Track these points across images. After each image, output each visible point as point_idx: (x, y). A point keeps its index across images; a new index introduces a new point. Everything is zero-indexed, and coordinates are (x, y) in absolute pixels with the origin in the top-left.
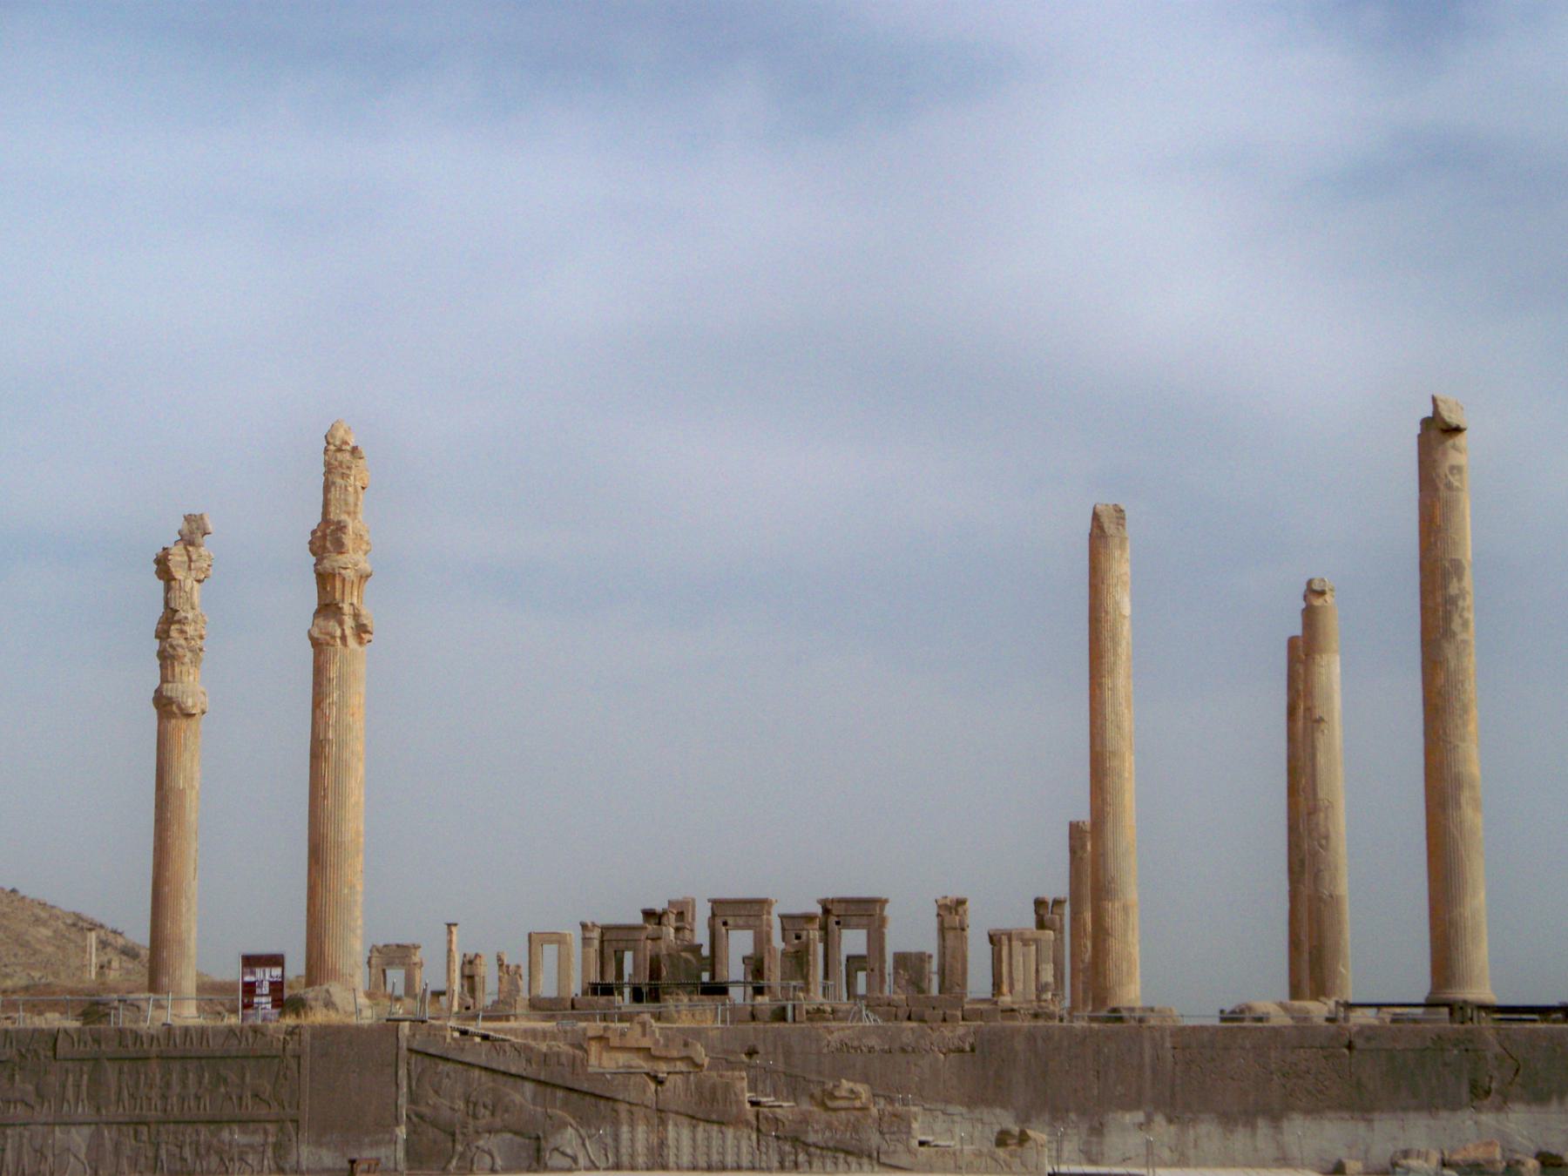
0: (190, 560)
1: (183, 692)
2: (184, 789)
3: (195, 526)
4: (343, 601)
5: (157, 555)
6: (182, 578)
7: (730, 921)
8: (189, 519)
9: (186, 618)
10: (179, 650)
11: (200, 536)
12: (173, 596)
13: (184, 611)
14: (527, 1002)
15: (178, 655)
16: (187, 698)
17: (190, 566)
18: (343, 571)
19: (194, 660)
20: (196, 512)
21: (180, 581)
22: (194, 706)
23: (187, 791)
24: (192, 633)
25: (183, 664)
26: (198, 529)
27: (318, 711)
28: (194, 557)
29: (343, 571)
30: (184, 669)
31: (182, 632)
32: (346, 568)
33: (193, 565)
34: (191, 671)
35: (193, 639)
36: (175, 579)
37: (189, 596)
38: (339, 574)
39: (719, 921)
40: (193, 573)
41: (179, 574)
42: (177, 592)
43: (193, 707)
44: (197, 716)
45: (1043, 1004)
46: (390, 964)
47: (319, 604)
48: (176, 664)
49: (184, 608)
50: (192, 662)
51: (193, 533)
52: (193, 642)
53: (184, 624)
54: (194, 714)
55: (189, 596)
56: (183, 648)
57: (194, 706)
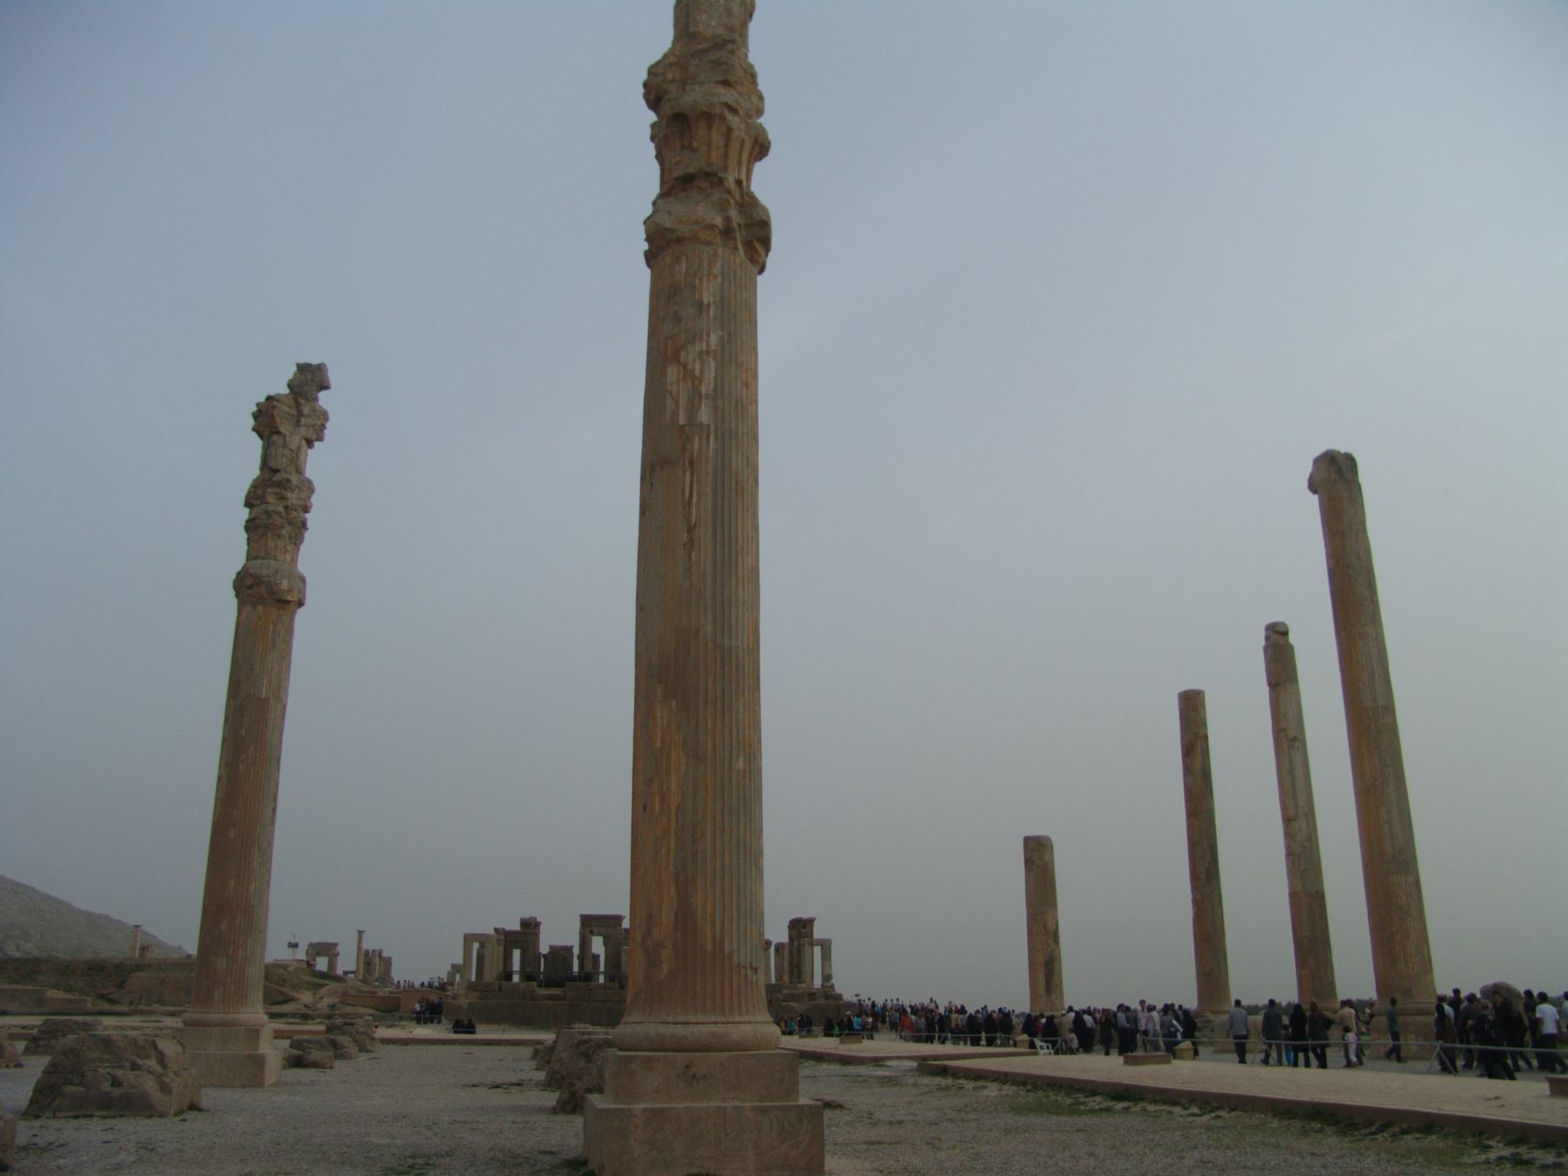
0: (300, 414)
1: (277, 571)
2: (267, 699)
3: (309, 377)
4: (725, 169)
5: (258, 405)
6: (287, 433)
7: (595, 930)
8: (303, 368)
9: (289, 481)
10: (276, 517)
11: (315, 388)
12: (274, 452)
13: (286, 472)
14: (466, 985)
15: (274, 524)
16: (282, 578)
17: (299, 421)
18: (729, 116)
19: (293, 534)
20: (314, 361)
21: (285, 436)
22: (290, 591)
23: (272, 703)
24: (295, 501)
25: (280, 537)
26: (312, 380)
27: (672, 372)
28: (306, 410)
29: (729, 116)
30: (280, 543)
31: (282, 498)
32: (734, 111)
33: (303, 420)
34: (289, 548)
35: (296, 510)
36: (278, 433)
37: (294, 455)
38: (722, 118)
39: (588, 930)
40: (303, 430)
41: (285, 428)
42: (280, 449)
43: (289, 591)
44: (292, 604)
45: (826, 989)
46: (320, 954)
47: (663, 183)
48: (270, 535)
49: (288, 469)
50: (290, 537)
51: (310, 380)
52: (294, 513)
53: (285, 489)
54: (288, 602)
55: (294, 455)
56: (282, 517)
57: (290, 591)
